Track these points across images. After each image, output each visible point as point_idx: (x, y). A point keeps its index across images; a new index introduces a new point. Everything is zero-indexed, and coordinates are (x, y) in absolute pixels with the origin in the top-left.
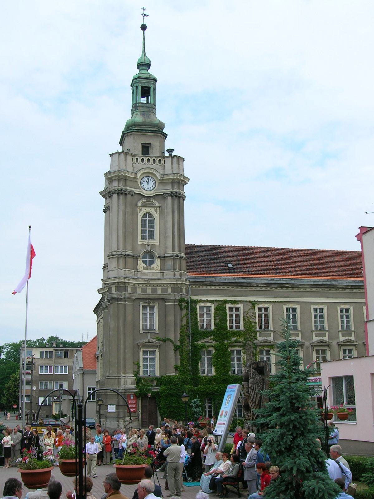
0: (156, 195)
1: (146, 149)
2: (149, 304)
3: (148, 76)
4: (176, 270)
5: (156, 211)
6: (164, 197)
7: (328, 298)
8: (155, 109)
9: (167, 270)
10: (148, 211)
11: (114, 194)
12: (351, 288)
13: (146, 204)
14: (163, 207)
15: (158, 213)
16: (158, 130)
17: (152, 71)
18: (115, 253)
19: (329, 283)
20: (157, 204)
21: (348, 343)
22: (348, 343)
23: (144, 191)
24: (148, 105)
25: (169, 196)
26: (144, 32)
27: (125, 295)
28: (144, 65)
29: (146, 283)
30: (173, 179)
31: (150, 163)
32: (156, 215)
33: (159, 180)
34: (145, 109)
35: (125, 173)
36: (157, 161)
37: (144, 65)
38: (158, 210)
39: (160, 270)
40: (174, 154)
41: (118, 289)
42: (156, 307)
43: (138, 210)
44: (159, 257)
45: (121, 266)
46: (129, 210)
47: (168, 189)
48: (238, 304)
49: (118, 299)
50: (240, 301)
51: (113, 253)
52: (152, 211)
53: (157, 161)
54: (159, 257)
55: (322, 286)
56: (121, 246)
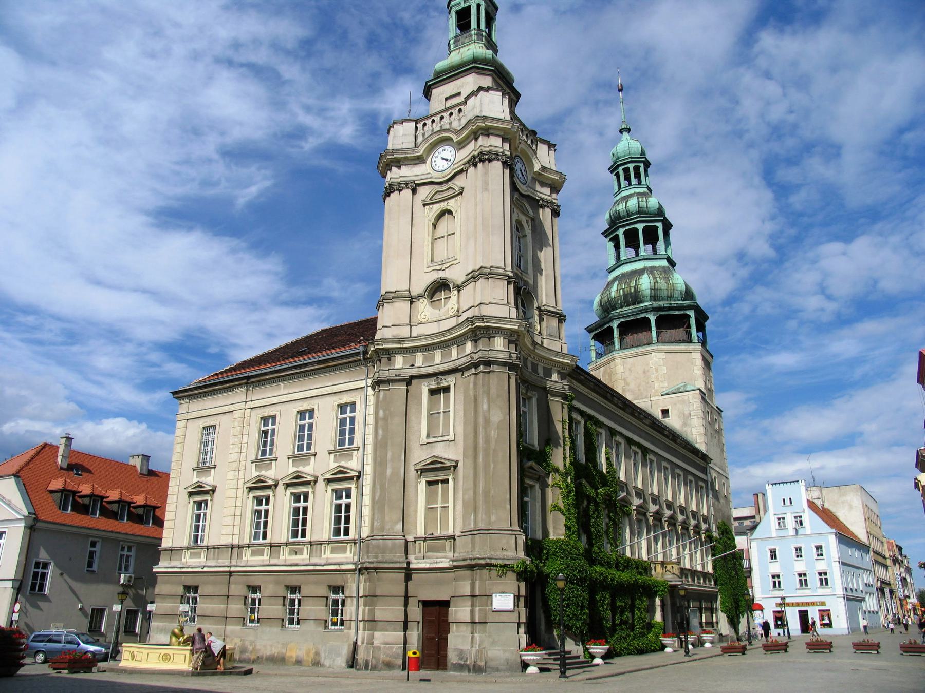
2: (527, 391)
18: (501, 271)
42: (534, 401)
51: (496, 270)
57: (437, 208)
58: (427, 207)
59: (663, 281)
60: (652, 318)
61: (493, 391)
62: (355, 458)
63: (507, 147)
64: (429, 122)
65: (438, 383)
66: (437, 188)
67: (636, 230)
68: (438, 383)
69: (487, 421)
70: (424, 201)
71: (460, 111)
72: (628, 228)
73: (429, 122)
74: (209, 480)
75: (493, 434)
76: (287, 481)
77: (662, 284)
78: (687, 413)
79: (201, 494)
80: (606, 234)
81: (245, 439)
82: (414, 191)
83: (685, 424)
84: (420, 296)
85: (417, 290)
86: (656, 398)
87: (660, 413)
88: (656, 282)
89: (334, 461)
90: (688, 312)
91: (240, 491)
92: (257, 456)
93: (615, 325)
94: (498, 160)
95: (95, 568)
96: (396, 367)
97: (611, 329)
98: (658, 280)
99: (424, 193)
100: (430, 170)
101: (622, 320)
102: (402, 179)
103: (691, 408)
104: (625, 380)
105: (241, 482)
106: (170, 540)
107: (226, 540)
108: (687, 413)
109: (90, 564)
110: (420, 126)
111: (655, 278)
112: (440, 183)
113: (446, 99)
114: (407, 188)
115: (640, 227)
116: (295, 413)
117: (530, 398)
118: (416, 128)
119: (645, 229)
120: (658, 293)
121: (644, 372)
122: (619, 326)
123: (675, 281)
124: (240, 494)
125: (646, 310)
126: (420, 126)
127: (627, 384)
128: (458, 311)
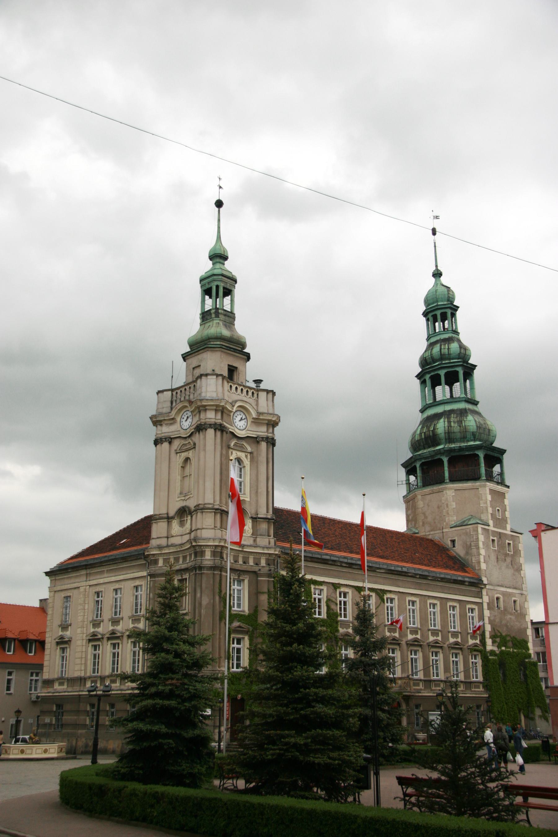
0: (248, 437)
1: (232, 370)
2: (239, 576)
3: (231, 276)
4: (270, 536)
5: (246, 456)
6: (256, 440)
7: (398, 586)
8: (235, 320)
9: (261, 535)
10: (238, 456)
11: (209, 428)
12: (419, 578)
13: (237, 446)
14: (255, 454)
15: (249, 460)
16: (236, 348)
17: (229, 265)
18: (210, 506)
19: (400, 569)
20: (249, 449)
21: (416, 643)
22: (416, 643)
23: (236, 430)
24: (230, 314)
25: (264, 441)
26: (219, 211)
27: (221, 563)
28: (218, 257)
29: (240, 549)
30: (269, 420)
31: (243, 395)
32: (247, 462)
33: (253, 418)
34: (227, 318)
35: (226, 404)
36: (250, 393)
37: (218, 257)
38: (249, 456)
39: (252, 534)
40: (262, 386)
41: (214, 554)
42: (246, 582)
43: (230, 452)
44: (252, 518)
45: (218, 525)
46: (224, 452)
47: (262, 431)
48: (322, 585)
49: (213, 568)
50: (324, 582)
52: (242, 455)
53: (250, 393)
54: (252, 518)
55: (396, 573)
56: (218, 498)
57: (184, 455)
58: (178, 455)
59: (456, 425)
60: (445, 460)
61: (204, 585)
62: (142, 622)
63: (219, 416)
64: (179, 391)
65: (182, 576)
66: (183, 442)
67: (439, 376)
68: (182, 576)
69: (200, 604)
70: (176, 450)
71: (194, 386)
72: (432, 374)
73: (179, 391)
74: (68, 634)
75: (203, 611)
76: (108, 636)
77: (455, 427)
78: (468, 543)
79: (63, 643)
80: (419, 376)
81: (86, 607)
82: (170, 443)
83: (467, 553)
84: (173, 518)
85: (172, 514)
86: (447, 530)
87: (449, 542)
88: (450, 426)
89: (132, 623)
90: (477, 452)
91: (85, 641)
92: (93, 618)
93: (418, 465)
94: (212, 428)
95: (12, 691)
96: (159, 565)
97: (415, 467)
98: (452, 424)
99: (176, 444)
100: (180, 429)
101: (423, 461)
102: (163, 435)
103: (472, 540)
104: (424, 514)
105: (85, 635)
106: (47, 674)
107: (77, 674)
108: (468, 543)
109: (8, 688)
110: (174, 393)
111: (449, 422)
112: (185, 438)
113: (194, 368)
114: (166, 441)
115: (442, 373)
116: (112, 590)
117: (243, 580)
118: (172, 394)
119: (446, 374)
120: (452, 436)
121: (438, 507)
122: (422, 465)
123: (467, 424)
124: (84, 644)
125: (439, 452)
126: (174, 393)
127: (426, 517)
128: (191, 530)
